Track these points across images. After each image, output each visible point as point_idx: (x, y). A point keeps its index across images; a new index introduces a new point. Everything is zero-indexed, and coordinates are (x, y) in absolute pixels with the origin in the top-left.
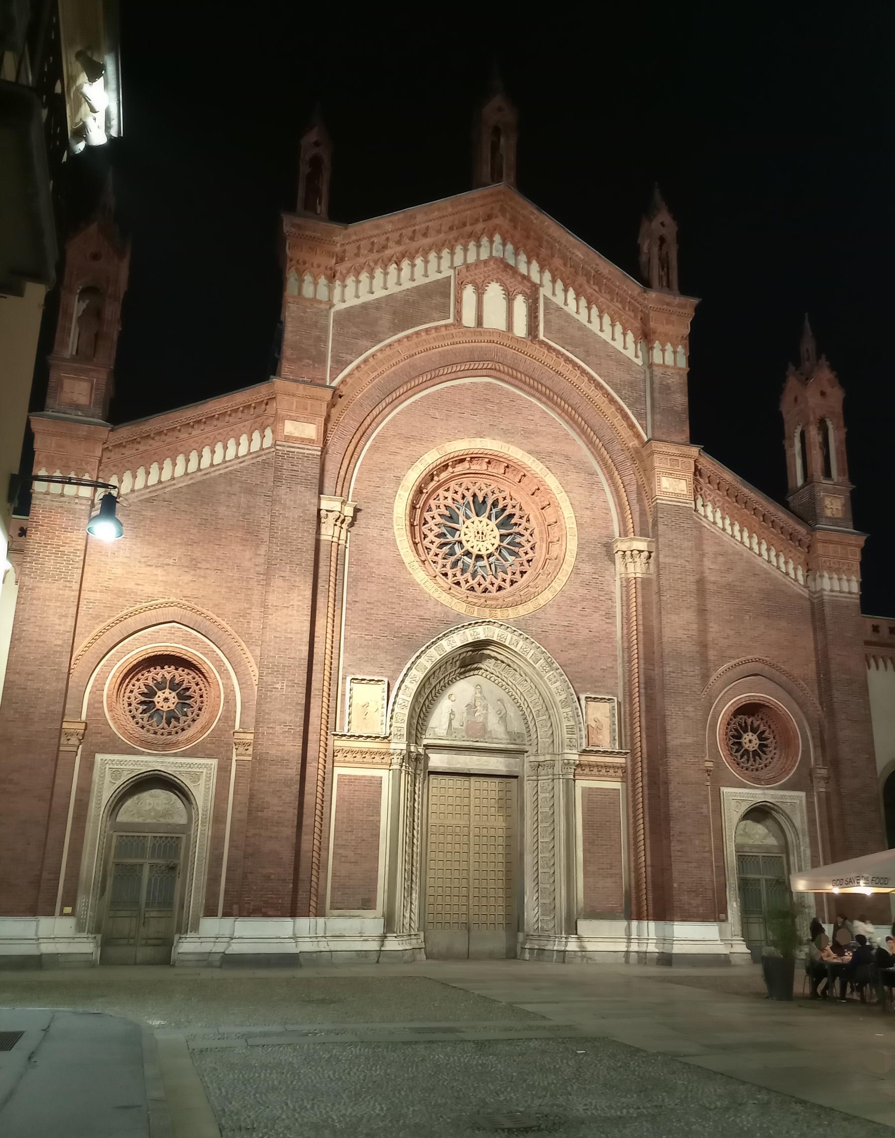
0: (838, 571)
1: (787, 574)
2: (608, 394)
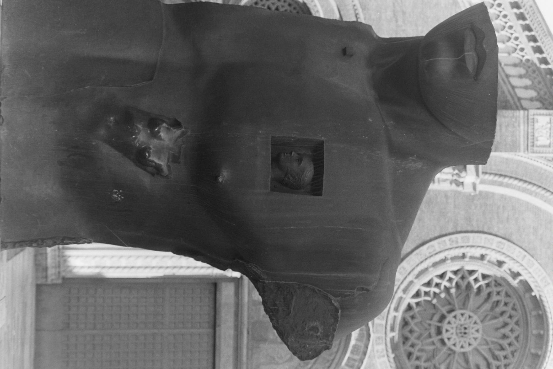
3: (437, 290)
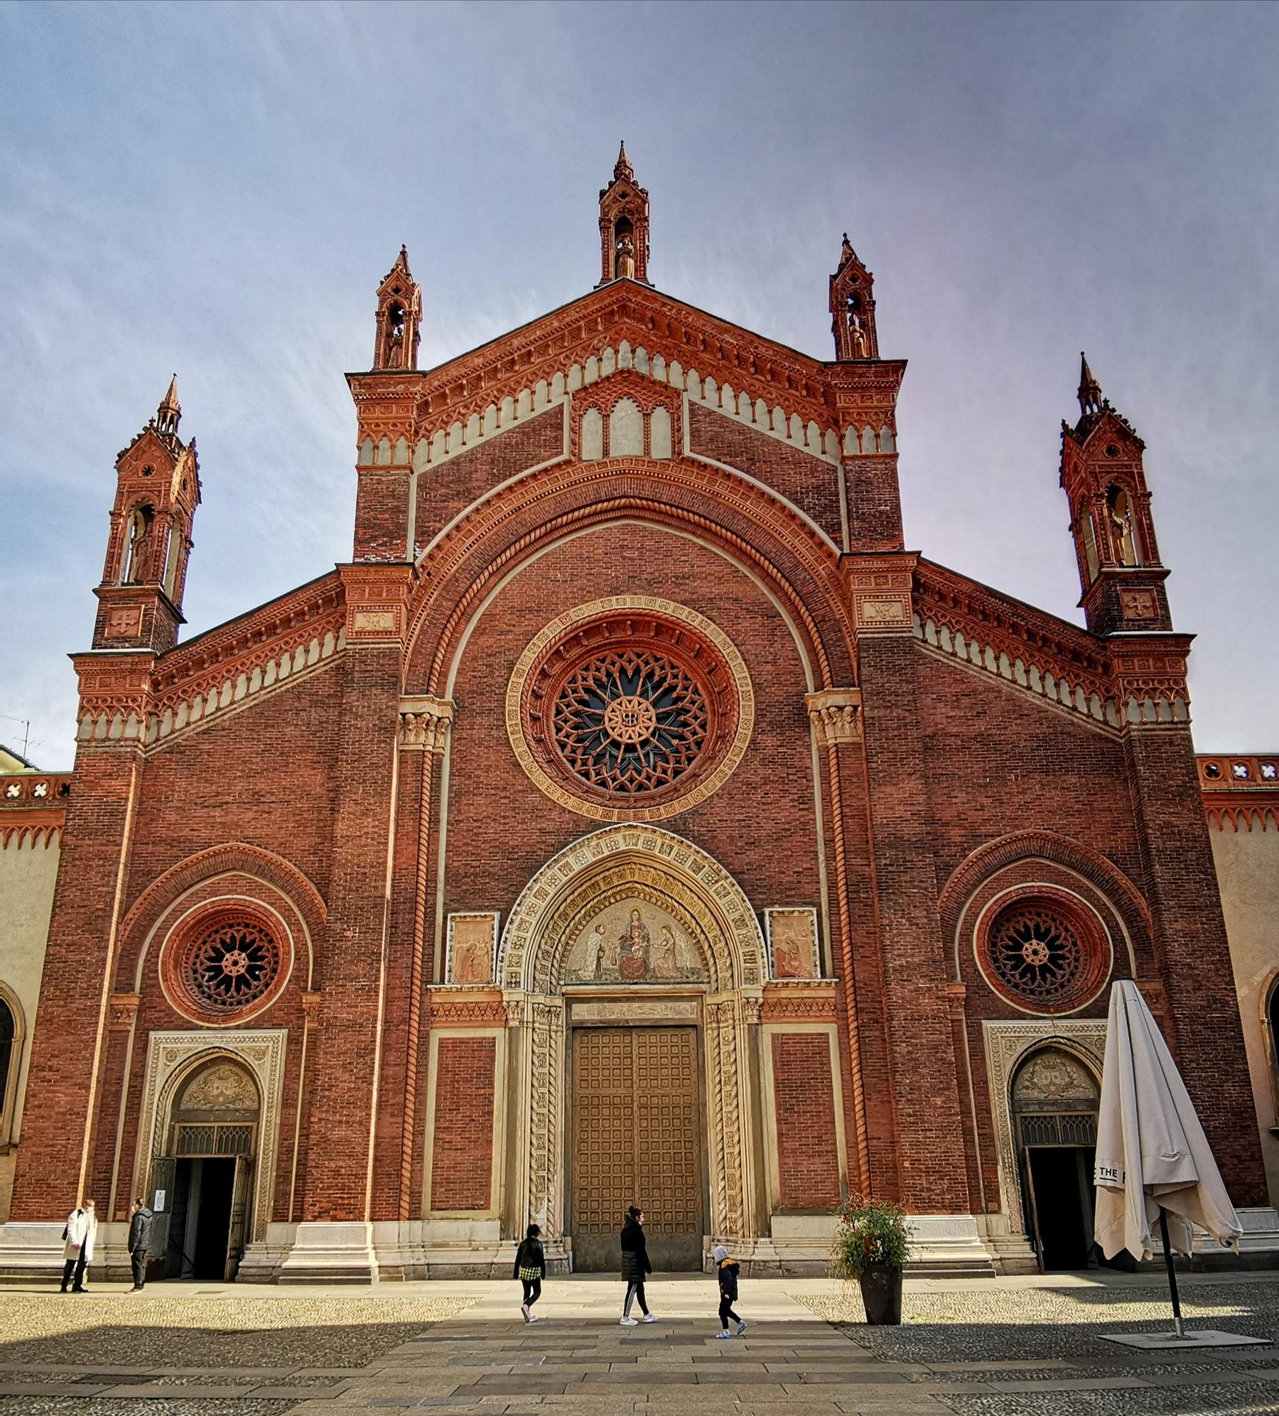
1: (1074, 708)
3: (579, 751)
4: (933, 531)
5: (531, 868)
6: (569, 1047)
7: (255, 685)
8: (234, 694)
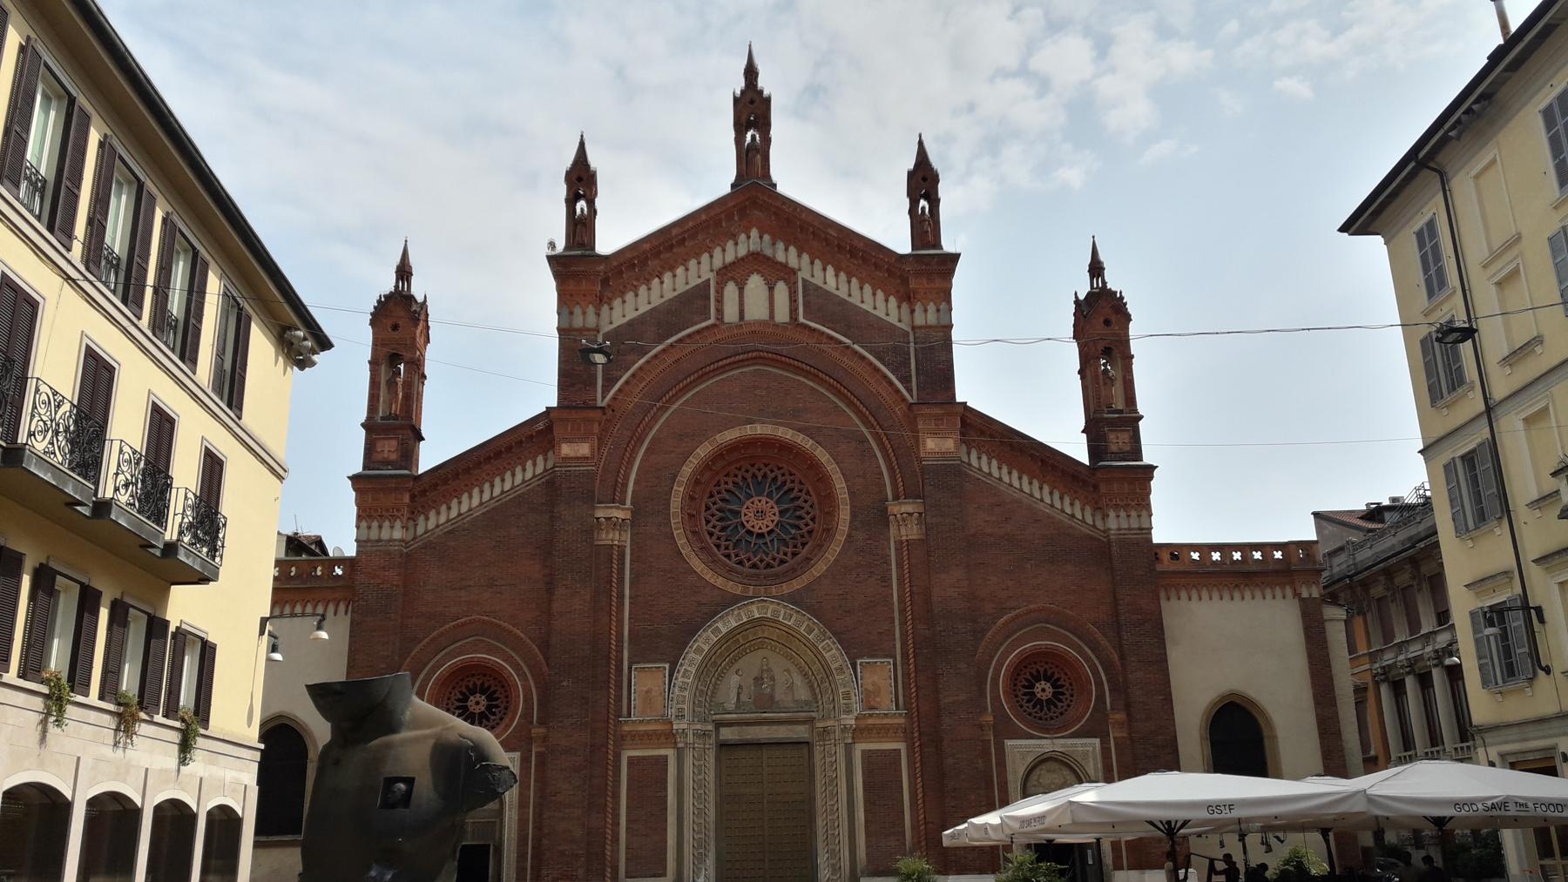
0: (1126, 507)
1: (1073, 516)
2: (871, 364)
4: (977, 385)
5: (691, 631)
6: (718, 759)
7: (486, 496)
8: (471, 502)
